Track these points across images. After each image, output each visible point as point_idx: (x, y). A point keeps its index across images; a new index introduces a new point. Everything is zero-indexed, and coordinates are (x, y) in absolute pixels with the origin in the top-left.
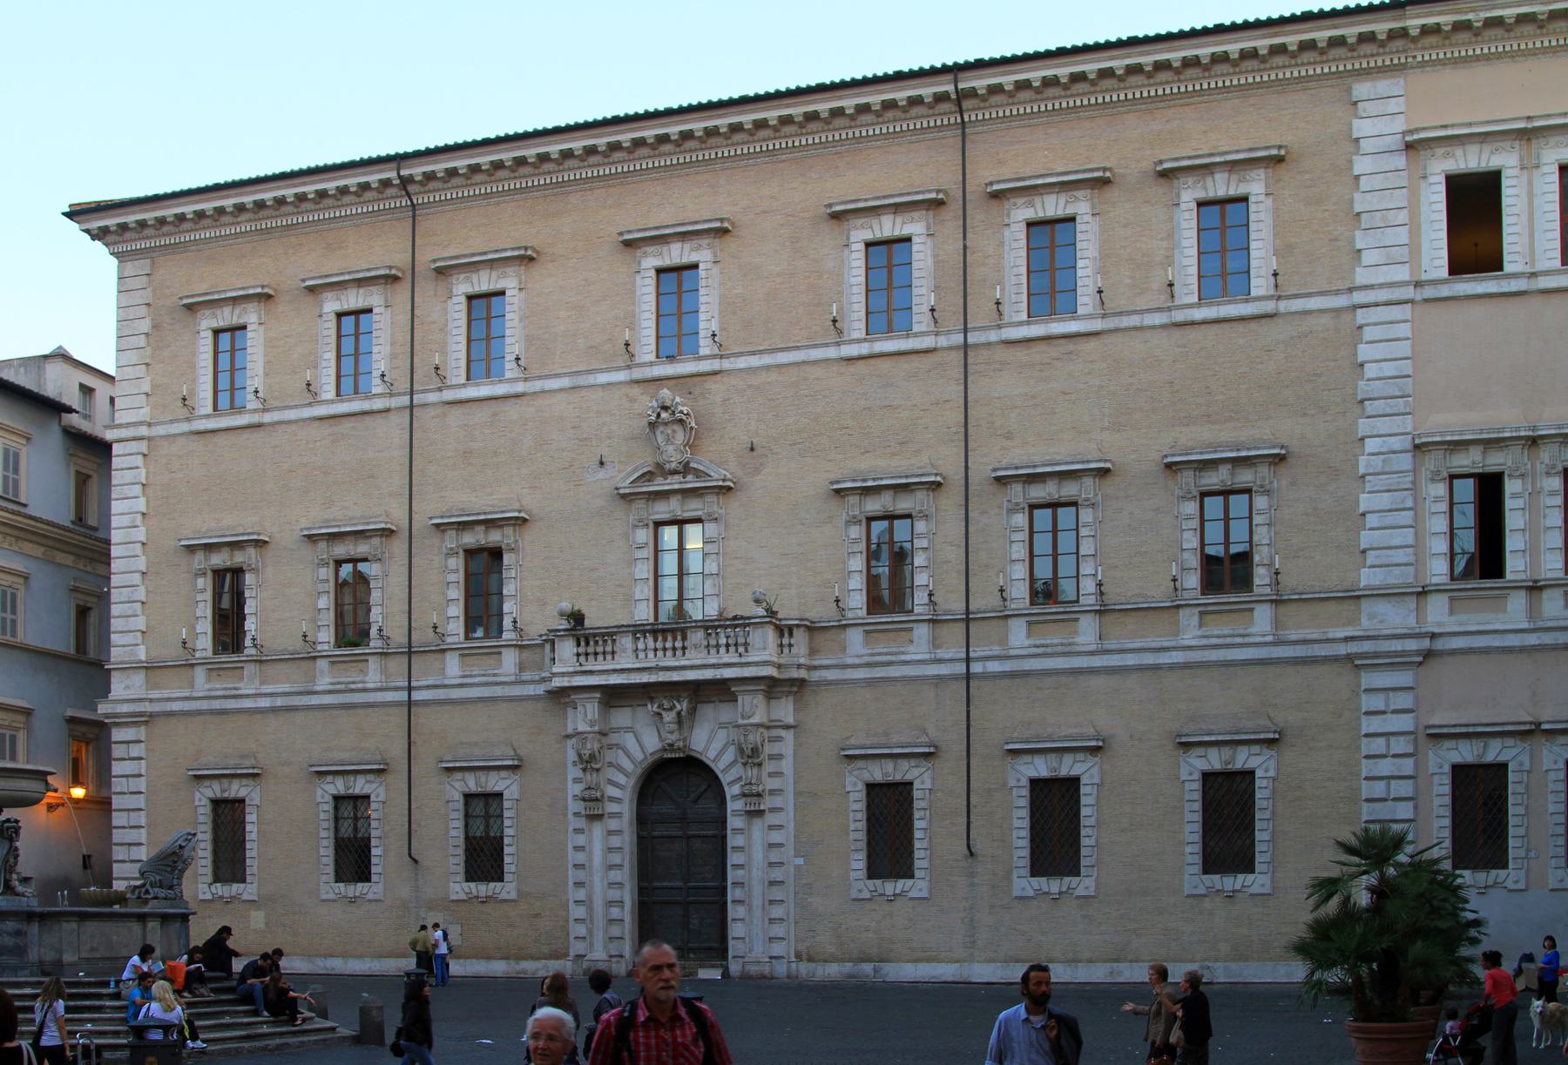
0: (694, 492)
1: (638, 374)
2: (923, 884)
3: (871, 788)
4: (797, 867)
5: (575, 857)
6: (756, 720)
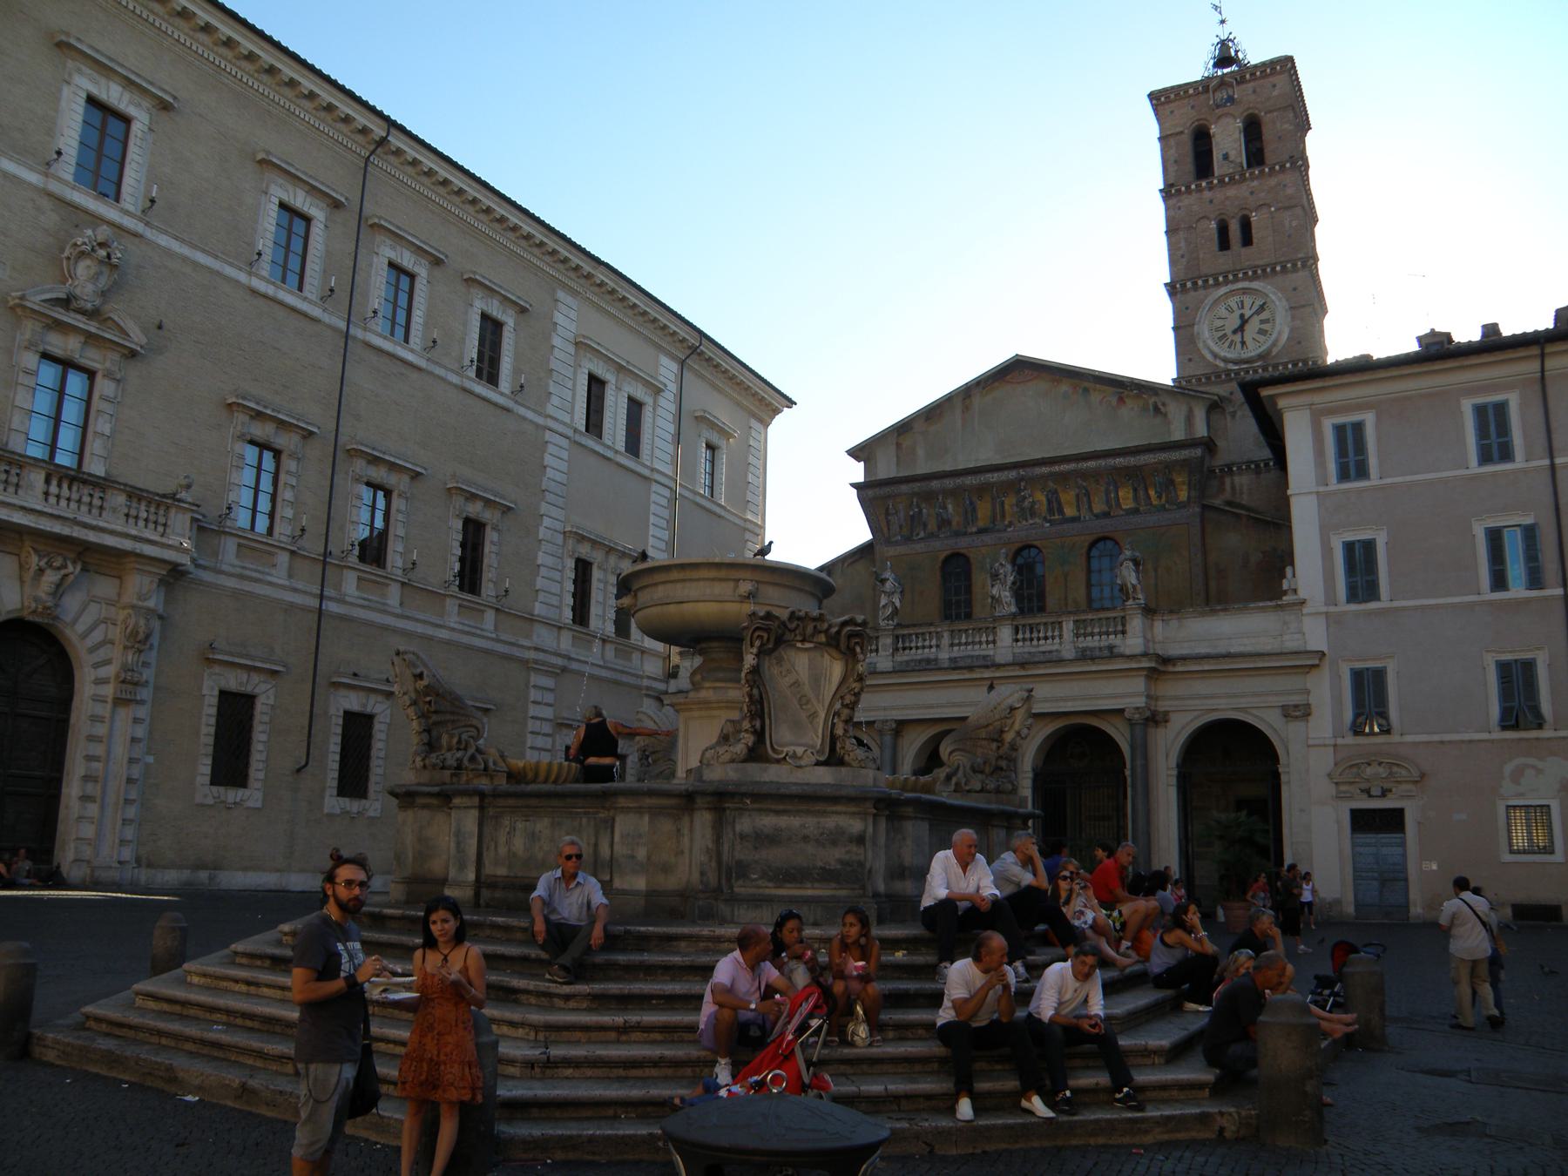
2: (259, 795)
4: (147, 765)
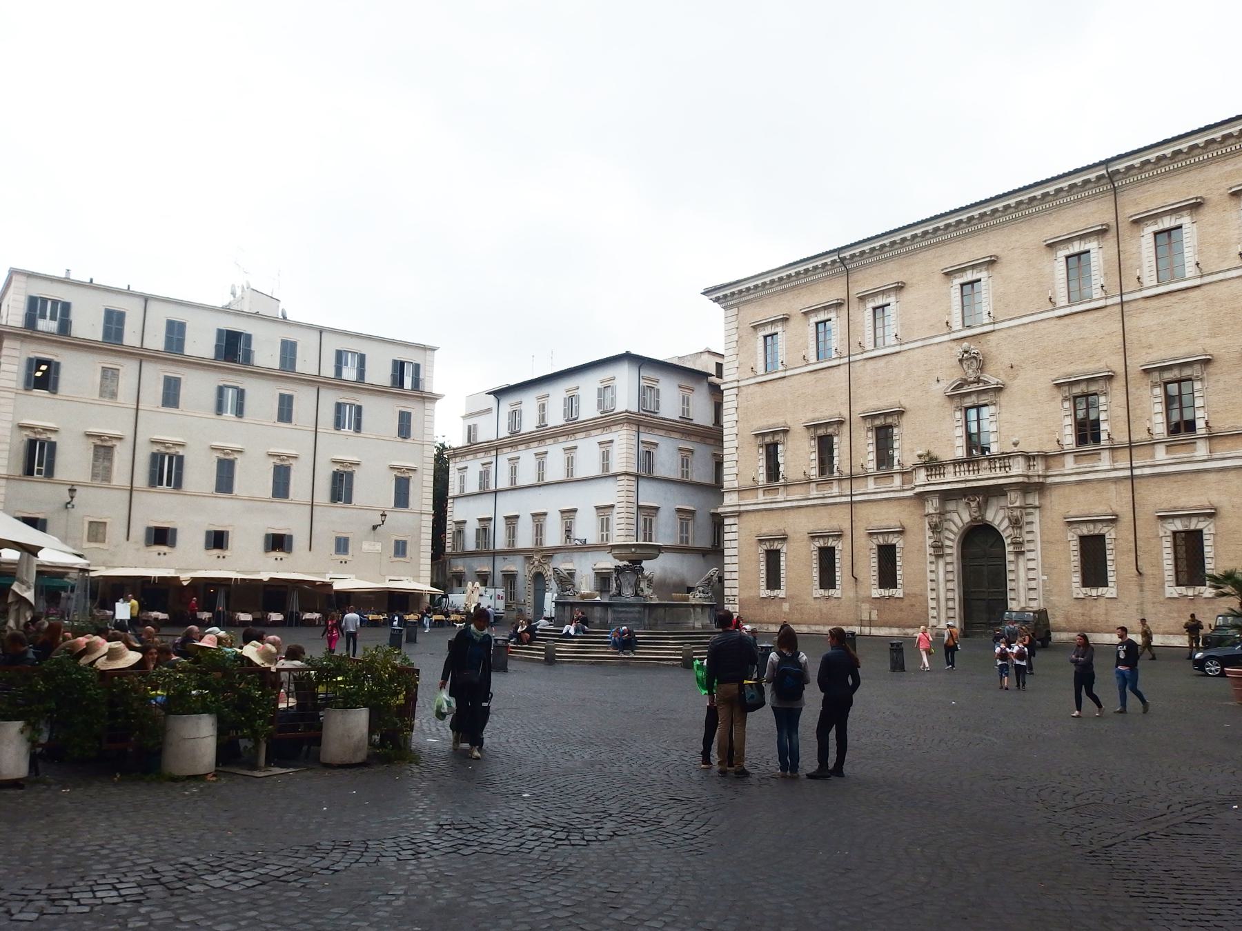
0: (979, 393)
1: (954, 336)
3: (1083, 539)
5: (931, 576)
6: (1017, 504)
